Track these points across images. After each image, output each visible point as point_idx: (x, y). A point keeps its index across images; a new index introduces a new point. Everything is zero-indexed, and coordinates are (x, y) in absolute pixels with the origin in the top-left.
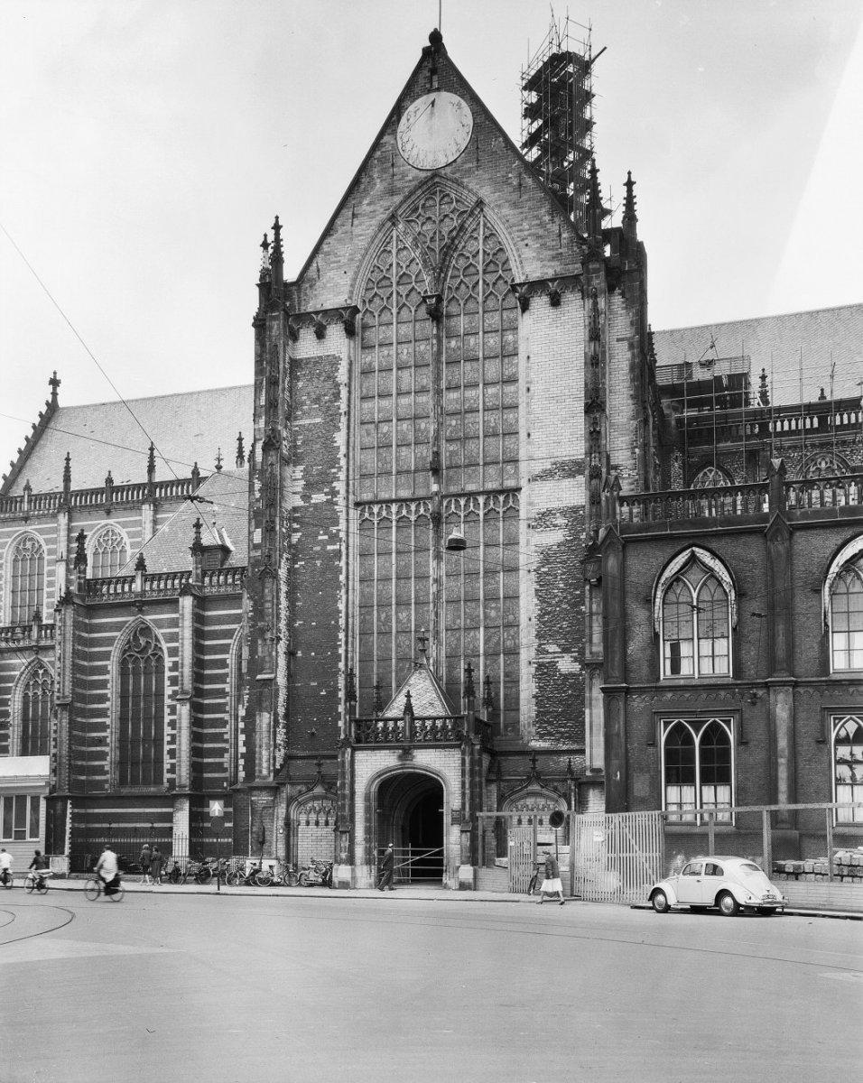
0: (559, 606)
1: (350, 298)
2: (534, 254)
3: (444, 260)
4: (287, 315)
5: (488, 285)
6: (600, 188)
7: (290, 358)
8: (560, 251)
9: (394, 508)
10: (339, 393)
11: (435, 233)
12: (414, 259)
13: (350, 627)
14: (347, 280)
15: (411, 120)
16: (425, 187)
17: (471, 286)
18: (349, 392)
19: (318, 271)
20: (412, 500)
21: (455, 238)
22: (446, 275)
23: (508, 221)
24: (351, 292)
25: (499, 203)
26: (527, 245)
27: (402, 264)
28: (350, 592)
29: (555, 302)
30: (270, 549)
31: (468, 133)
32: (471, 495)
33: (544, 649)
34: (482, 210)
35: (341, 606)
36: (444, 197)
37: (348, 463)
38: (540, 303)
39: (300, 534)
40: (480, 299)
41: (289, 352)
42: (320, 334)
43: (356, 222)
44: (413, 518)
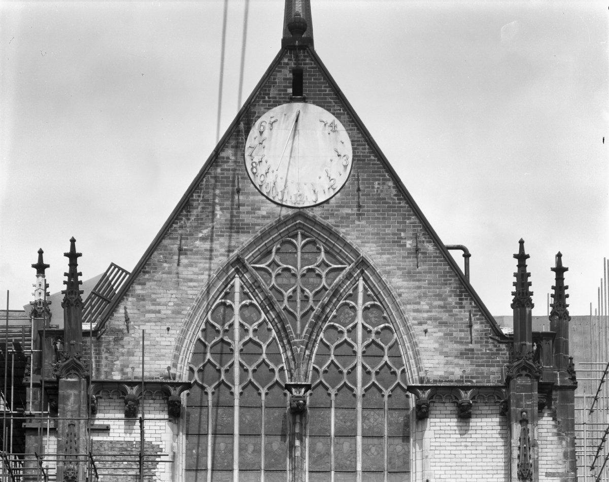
2: (436, 345)
5: (369, 373)
6: (529, 279)
8: (471, 346)
11: (295, 291)
14: (169, 341)
15: (266, 134)
17: (345, 371)
19: (127, 320)
21: (327, 305)
22: (312, 352)
23: (400, 295)
24: (176, 357)
25: (388, 268)
26: (426, 331)
27: (247, 326)
29: (464, 414)
31: (345, 167)
34: (362, 272)
40: (359, 391)
43: (184, 261)
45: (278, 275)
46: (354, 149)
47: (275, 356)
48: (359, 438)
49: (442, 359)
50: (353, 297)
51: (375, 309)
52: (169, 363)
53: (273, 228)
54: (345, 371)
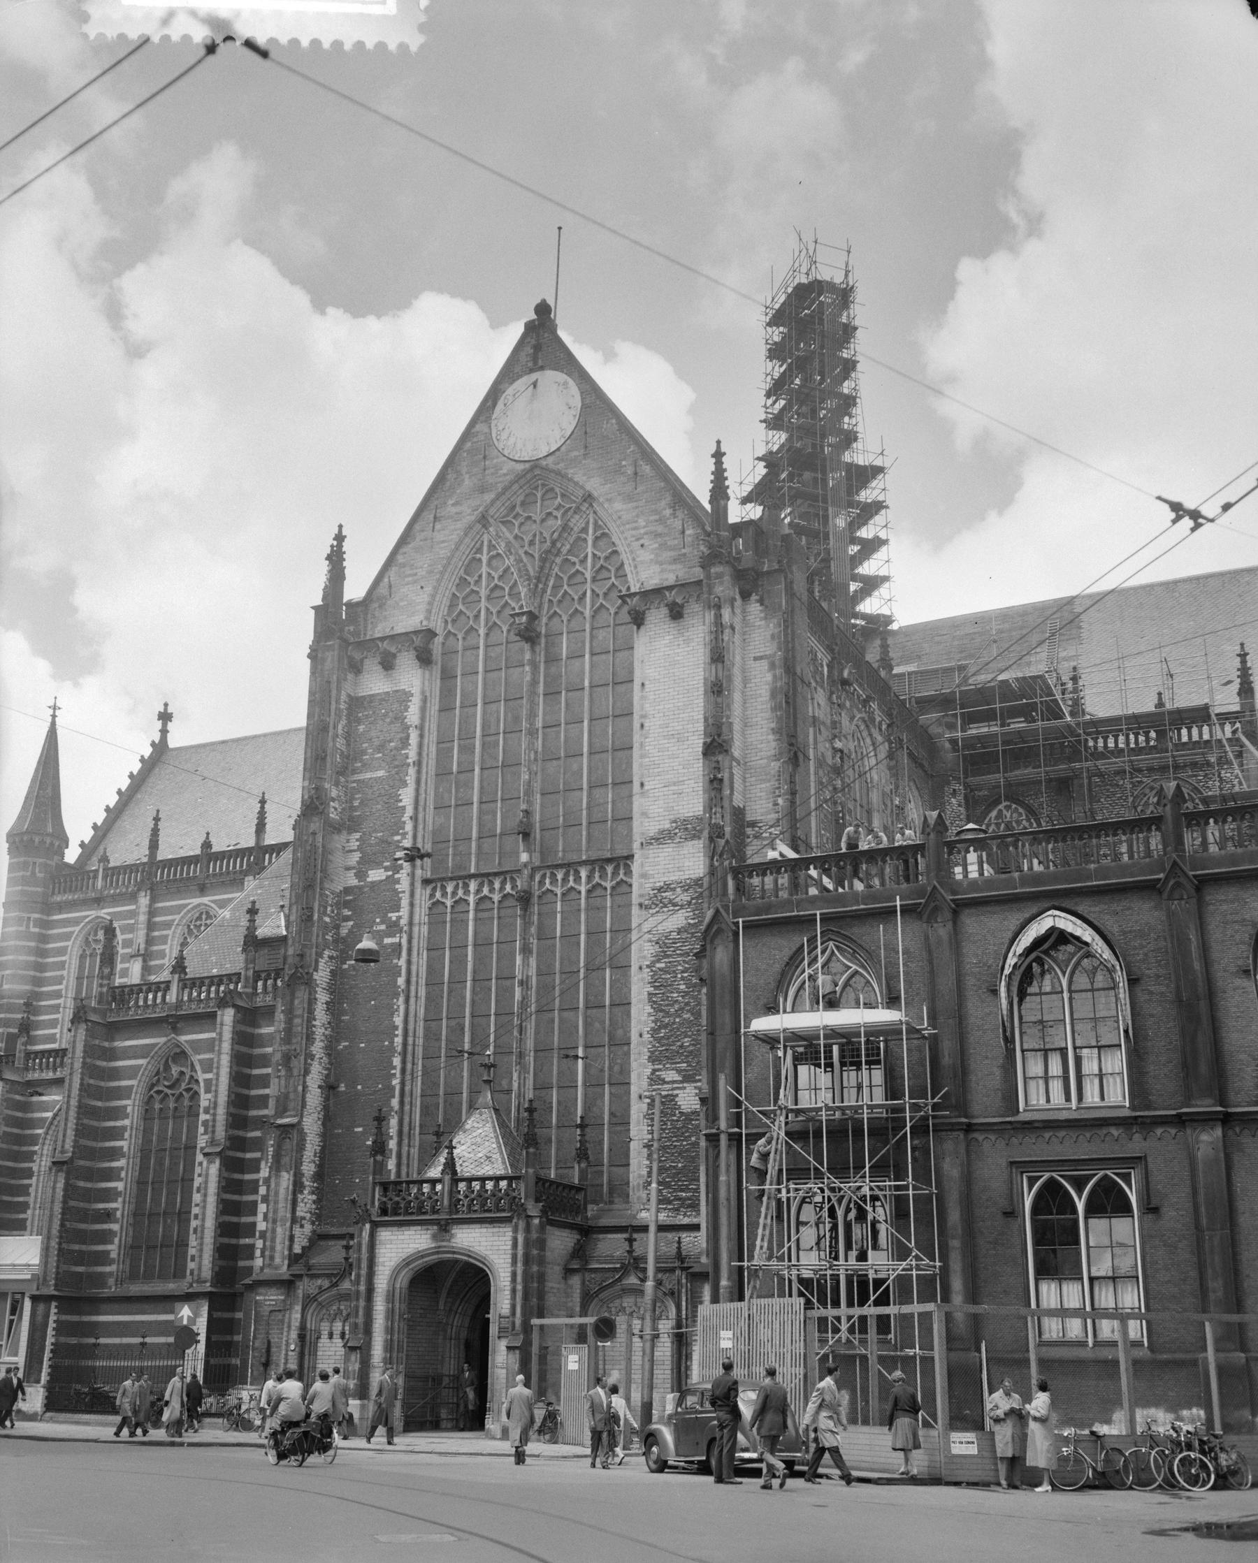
0: (679, 1016)
1: (427, 618)
2: (652, 556)
3: (542, 568)
4: (345, 643)
6: (726, 474)
7: (349, 696)
8: (683, 551)
9: (473, 886)
10: (408, 737)
11: (535, 535)
12: (508, 568)
13: (410, 1048)
14: (423, 597)
16: (522, 481)
18: (421, 736)
19: (390, 587)
20: (496, 874)
22: (546, 585)
24: (429, 611)
27: (493, 573)
28: (412, 1000)
30: (304, 946)
32: (571, 867)
33: (659, 1077)
34: (591, 505)
35: (398, 1020)
36: (547, 491)
37: (415, 828)
38: (657, 617)
39: (351, 923)
41: (348, 689)
42: (388, 664)
44: (496, 897)
45: (522, 524)
46: (583, 399)
47: (515, 595)
48: (587, 656)
49: (657, 568)
50: (585, 530)
51: (600, 537)
52: (422, 617)
53: (512, 483)
54: (576, 598)
